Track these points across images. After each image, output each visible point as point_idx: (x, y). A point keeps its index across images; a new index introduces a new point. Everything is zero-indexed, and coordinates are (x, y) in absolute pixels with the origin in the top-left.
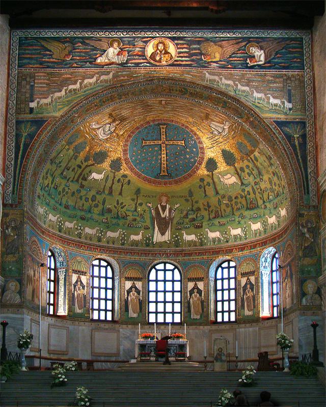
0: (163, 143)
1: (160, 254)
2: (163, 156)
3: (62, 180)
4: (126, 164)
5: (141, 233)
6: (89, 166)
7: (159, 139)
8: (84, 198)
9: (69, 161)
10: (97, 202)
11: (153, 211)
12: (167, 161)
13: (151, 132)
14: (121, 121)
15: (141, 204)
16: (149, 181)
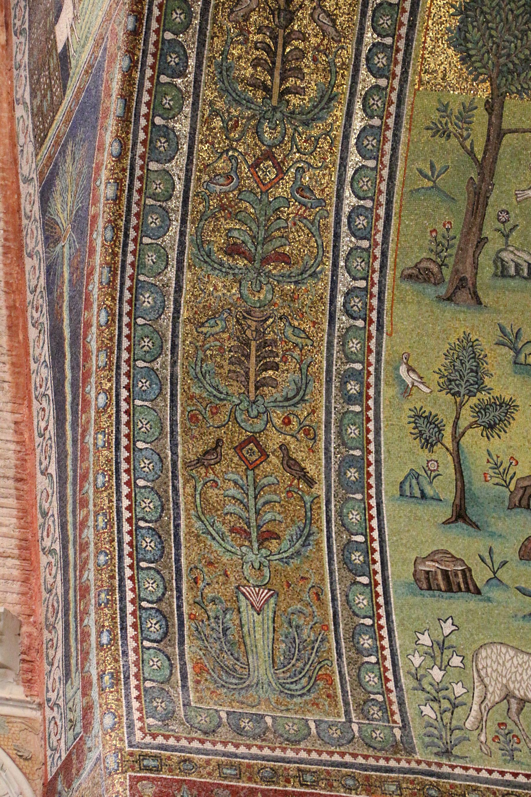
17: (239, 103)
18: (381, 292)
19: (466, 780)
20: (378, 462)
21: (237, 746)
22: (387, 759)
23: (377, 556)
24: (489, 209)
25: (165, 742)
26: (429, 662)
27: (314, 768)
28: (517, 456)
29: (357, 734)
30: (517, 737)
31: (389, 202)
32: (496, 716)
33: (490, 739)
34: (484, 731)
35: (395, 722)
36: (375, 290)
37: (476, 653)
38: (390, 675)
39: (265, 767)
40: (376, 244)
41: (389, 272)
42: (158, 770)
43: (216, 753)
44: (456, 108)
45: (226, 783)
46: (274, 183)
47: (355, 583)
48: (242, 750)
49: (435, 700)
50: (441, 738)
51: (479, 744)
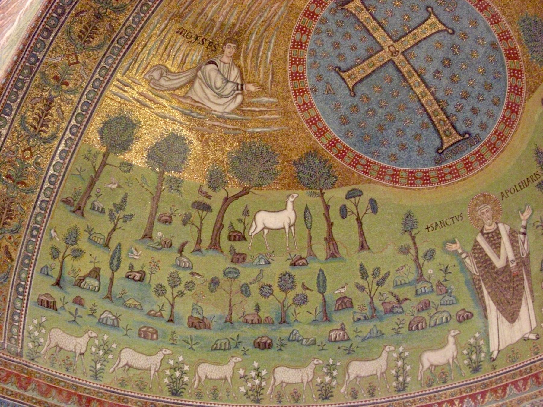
0: (394, 53)
1: (515, 384)
2: (418, 91)
3: (156, 255)
4: (342, 157)
5: (451, 340)
6: (236, 197)
7: (378, 48)
8: (254, 289)
9: (156, 199)
10: (299, 289)
11: (467, 260)
12: (438, 101)
13: (338, 37)
14: (238, 43)
15: (430, 255)
16: (426, 179)
17: (25, 130)
18: (53, 204)
20: (36, 259)
22: (14, 358)
23: (27, 290)
24: (95, 187)
26: (35, 329)
28: (81, 269)
31: (64, 175)
32: (52, 351)
36: (51, 202)
37: (51, 330)
38: (21, 330)
40: (56, 188)
41: (57, 198)
44: (93, 152)
46: (28, 159)
47: (18, 298)
49: (33, 342)
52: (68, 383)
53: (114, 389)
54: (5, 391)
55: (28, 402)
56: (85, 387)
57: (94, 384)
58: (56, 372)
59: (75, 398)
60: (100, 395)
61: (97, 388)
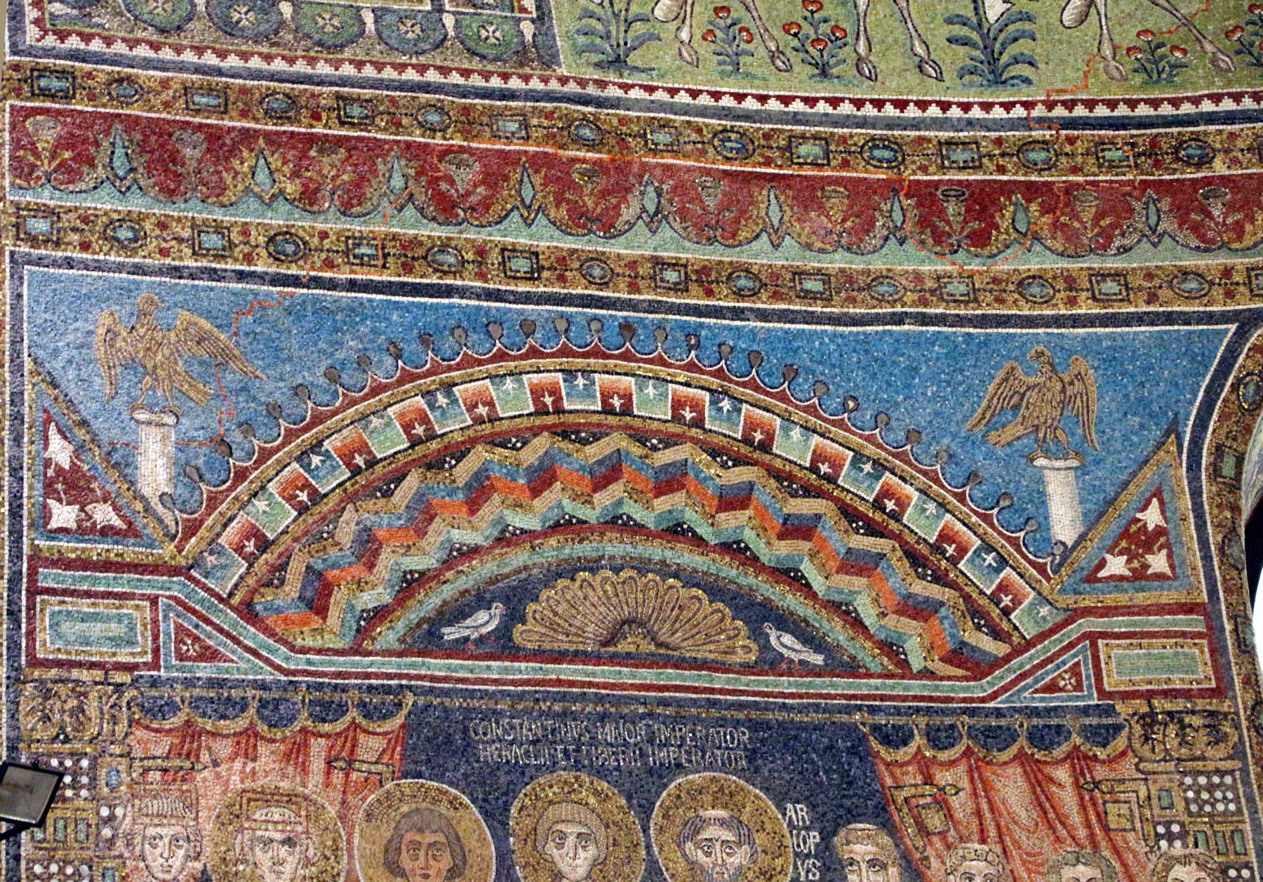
19: (649, 110)
21: (222, 55)
22: (505, 77)
25: (82, 46)
27: (367, 93)
29: (451, 33)
30: (747, 30)
33: (698, 36)
34: (688, 22)
35: (523, 10)
39: (275, 92)
42: (68, 97)
43: (181, 67)
45: (197, 120)
48: (233, 61)
50: (608, 38)
51: (678, 45)
52: (843, 139)
53: (1112, 104)
54: (494, 257)
55: (634, 288)
56: (944, 135)
57: (987, 107)
58: (763, 99)
59: (900, 210)
60: (1039, 156)
61: (1013, 124)
